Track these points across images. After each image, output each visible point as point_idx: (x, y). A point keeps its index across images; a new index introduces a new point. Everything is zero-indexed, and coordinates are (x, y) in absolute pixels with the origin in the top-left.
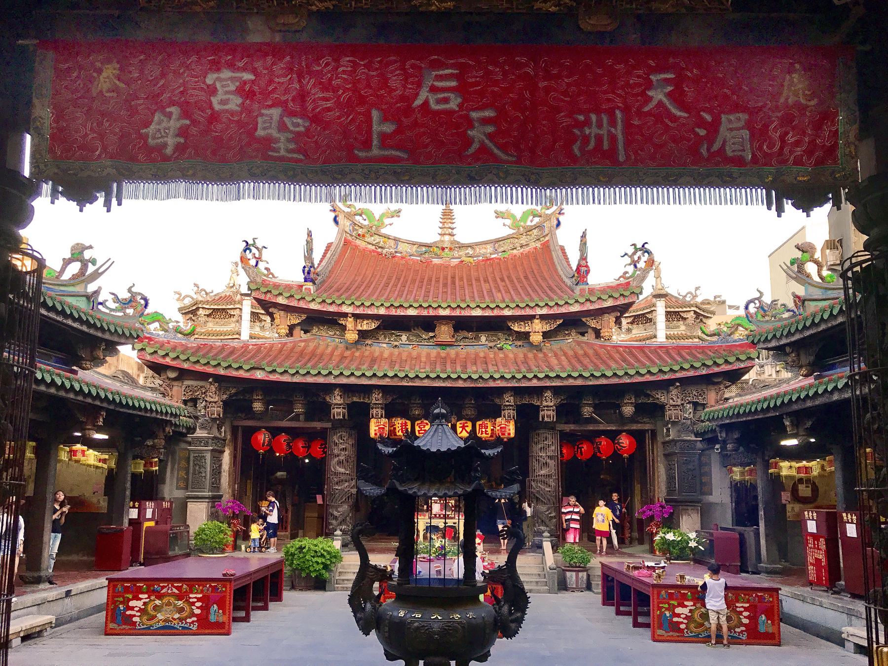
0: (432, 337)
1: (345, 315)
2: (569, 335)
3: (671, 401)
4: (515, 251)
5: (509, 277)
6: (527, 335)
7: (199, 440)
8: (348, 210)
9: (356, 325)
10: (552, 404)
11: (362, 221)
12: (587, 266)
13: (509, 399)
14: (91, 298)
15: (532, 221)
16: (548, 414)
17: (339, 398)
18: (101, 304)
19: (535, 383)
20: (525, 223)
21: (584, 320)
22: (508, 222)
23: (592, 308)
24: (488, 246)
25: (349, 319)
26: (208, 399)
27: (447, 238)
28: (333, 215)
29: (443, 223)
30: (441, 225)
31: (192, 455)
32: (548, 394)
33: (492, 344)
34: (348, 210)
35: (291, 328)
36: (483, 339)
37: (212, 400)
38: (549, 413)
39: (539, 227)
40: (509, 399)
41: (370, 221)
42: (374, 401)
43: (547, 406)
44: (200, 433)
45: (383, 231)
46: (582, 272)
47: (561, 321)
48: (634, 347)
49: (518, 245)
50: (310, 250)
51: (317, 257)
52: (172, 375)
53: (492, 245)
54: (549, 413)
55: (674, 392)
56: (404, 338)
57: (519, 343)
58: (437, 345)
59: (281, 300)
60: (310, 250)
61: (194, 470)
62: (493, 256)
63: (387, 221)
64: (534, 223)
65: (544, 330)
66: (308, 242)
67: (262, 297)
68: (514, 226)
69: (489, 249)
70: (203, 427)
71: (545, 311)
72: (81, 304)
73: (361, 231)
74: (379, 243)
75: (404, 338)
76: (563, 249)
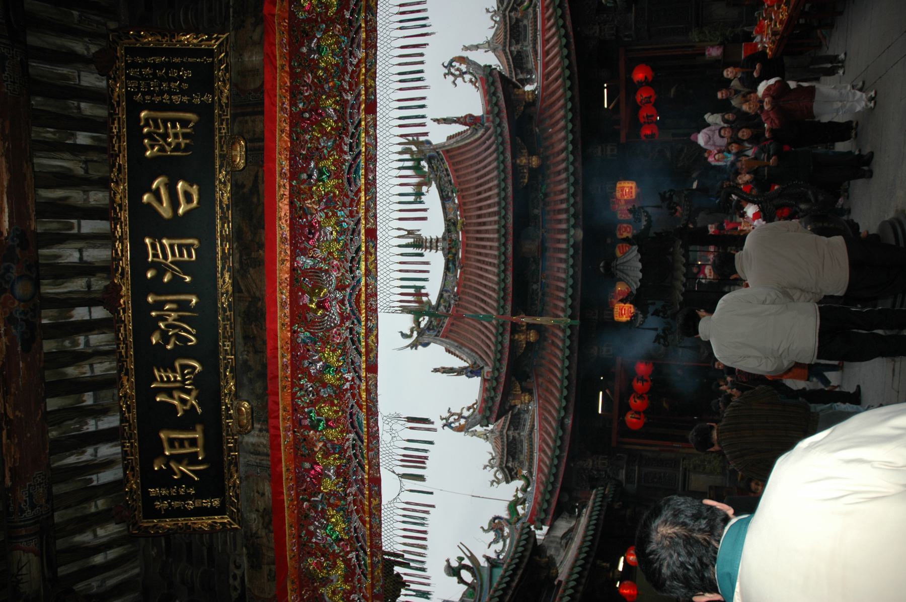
5: (477, 187)
6: (531, 170)
12: (466, 117)
14: (493, 563)
18: (498, 556)
21: (516, 118)
25: (516, 337)
28: (420, 347)
36: (536, 211)
37: (591, 464)
44: (622, 475)
46: (470, 120)
47: (518, 138)
48: (544, 70)
49: (446, 179)
50: (451, 371)
51: (458, 363)
56: (535, 287)
60: (451, 371)
66: (443, 372)
67: (494, 416)
72: (499, 572)
74: (445, 307)
75: (535, 287)
76: (450, 138)
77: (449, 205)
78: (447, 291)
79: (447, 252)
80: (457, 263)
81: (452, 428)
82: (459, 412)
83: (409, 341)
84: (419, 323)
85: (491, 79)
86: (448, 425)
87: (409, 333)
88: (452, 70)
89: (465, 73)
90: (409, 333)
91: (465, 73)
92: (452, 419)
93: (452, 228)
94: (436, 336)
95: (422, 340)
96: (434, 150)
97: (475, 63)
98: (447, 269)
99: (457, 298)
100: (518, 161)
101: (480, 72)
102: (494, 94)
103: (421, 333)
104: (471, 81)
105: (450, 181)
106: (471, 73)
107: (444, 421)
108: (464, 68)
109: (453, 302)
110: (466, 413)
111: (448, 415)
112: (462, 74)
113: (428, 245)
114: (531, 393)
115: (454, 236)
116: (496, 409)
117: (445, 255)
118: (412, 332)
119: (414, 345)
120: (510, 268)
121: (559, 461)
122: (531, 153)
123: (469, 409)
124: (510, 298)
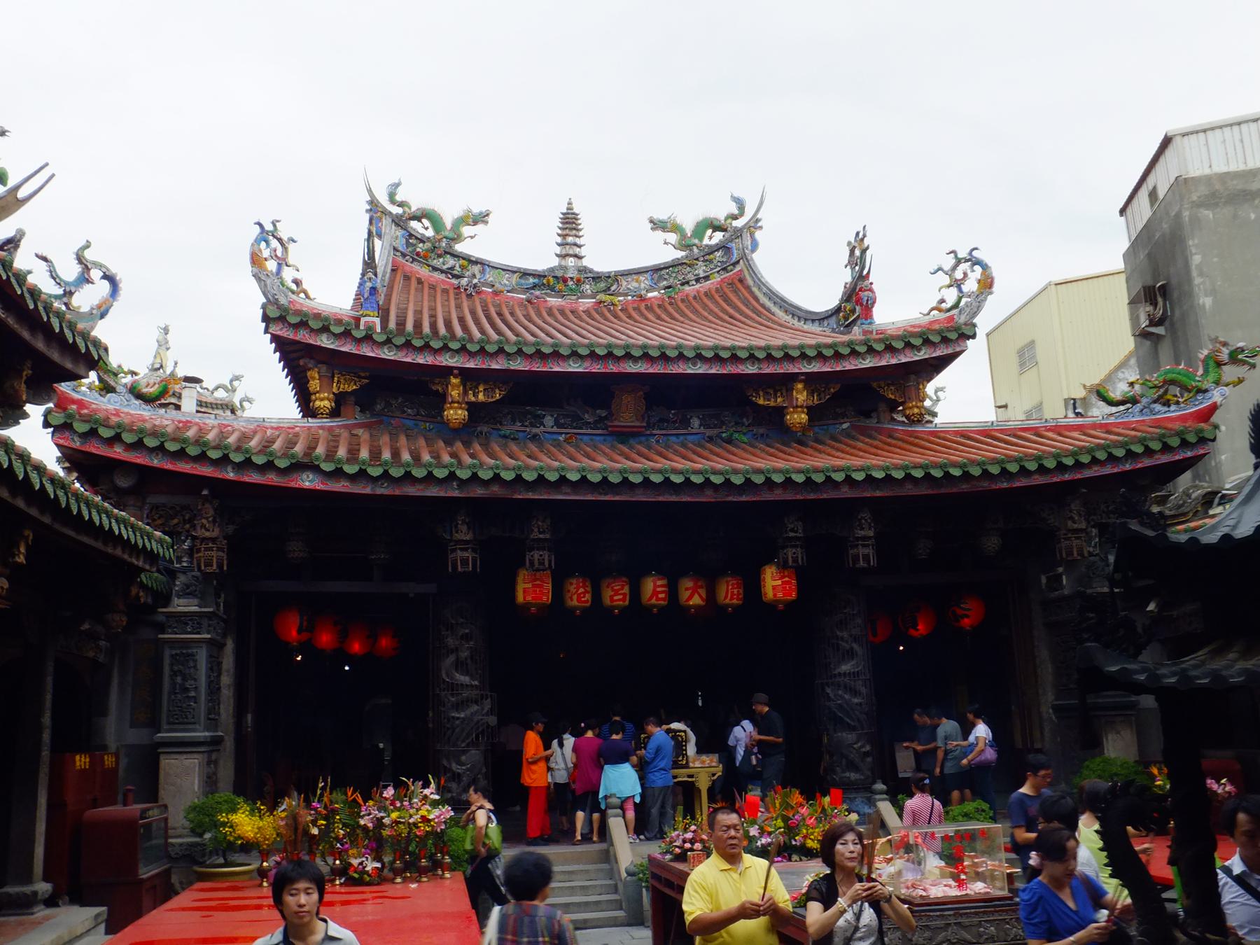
0: (601, 419)
1: (448, 371)
2: (844, 415)
3: (1070, 523)
4: (687, 288)
6: (780, 412)
7: (183, 620)
8: (399, 210)
9: (465, 393)
10: (871, 533)
11: (422, 231)
13: (794, 528)
15: (711, 238)
16: (865, 554)
17: (464, 528)
19: (846, 493)
20: (701, 239)
21: (875, 385)
22: (673, 237)
23: (894, 361)
24: (642, 278)
25: (454, 381)
26: (200, 533)
27: (571, 262)
29: (564, 236)
30: (559, 240)
31: (167, 653)
32: (866, 515)
33: (709, 432)
34: (399, 210)
35: (340, 399)
36: (696, 422)
38: (866, 551)
39: (723, 247)
40: (794, 528)
41: (437, 231)
42: (536, 535)
43: (865, 538)
44: (181, 605)
45: (459, 248)
47: (838, 387)
52: (123, 482)
53: (648, 275)
54: (866, 551)
55: (1076, 506)
56: (549, 421)
57: (761, 431)
58: (611, 434)
59: (325, 342)
61: (174, 684)
62: (650, 295)
63: (466, 230)
64: (715, 241)
65: (810, 403)
68: (684, 245)
69: (645, 282)
70: (186, 593)
71: (815, 367)
73: (420, 248)
74: (452, 268)
75: (549, 421)
77: (645, 282)
78: (483, 272)
79: (559, 274)
80: (537, 293)
81: (257, 241)
82: (290, 261)
83: (383, 200)
84: (419, 219)
85: (953, 336)
86: (265, 235)
87: (398, 198)
88: (964, 266)
89: (960, 290)
90: (398, 198)
91: (960, 290)
92: (274, 243)
93: (602, 285)
94: (395, 249)
95: (386, 222)
96: (744, 257)
97: (979, 308)
98: (525, 274)
99: (470, 290)
100: (800, 386)
101: (963, 319)
102: (927, 342)
103: (399, 222)
104: (942, 301)
105: (687, 283)
106: (960, 299)
107: (269, 227)
108: (971, 286)
109: (464, 281)
110: (288, 275)
111: (285, 238)
112: (957, 284)
113: (570, 239)
114: (335, 413)
115: (587, 288)
116: (303, 336)
117: (552, 270)
118: (401, 205)
119: (374, 206)
120: (597, 368)
121: (215, 463)
122: (811, 411)
123: (297, 282)
124: (538, 367)
